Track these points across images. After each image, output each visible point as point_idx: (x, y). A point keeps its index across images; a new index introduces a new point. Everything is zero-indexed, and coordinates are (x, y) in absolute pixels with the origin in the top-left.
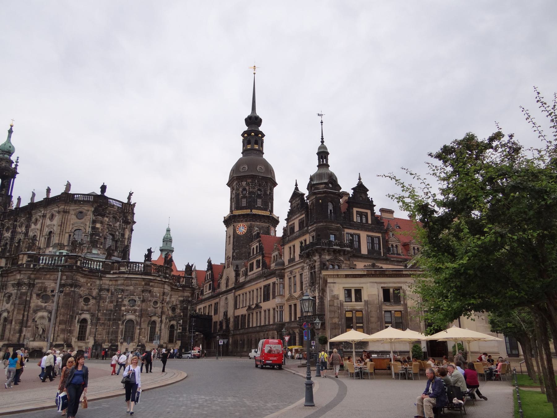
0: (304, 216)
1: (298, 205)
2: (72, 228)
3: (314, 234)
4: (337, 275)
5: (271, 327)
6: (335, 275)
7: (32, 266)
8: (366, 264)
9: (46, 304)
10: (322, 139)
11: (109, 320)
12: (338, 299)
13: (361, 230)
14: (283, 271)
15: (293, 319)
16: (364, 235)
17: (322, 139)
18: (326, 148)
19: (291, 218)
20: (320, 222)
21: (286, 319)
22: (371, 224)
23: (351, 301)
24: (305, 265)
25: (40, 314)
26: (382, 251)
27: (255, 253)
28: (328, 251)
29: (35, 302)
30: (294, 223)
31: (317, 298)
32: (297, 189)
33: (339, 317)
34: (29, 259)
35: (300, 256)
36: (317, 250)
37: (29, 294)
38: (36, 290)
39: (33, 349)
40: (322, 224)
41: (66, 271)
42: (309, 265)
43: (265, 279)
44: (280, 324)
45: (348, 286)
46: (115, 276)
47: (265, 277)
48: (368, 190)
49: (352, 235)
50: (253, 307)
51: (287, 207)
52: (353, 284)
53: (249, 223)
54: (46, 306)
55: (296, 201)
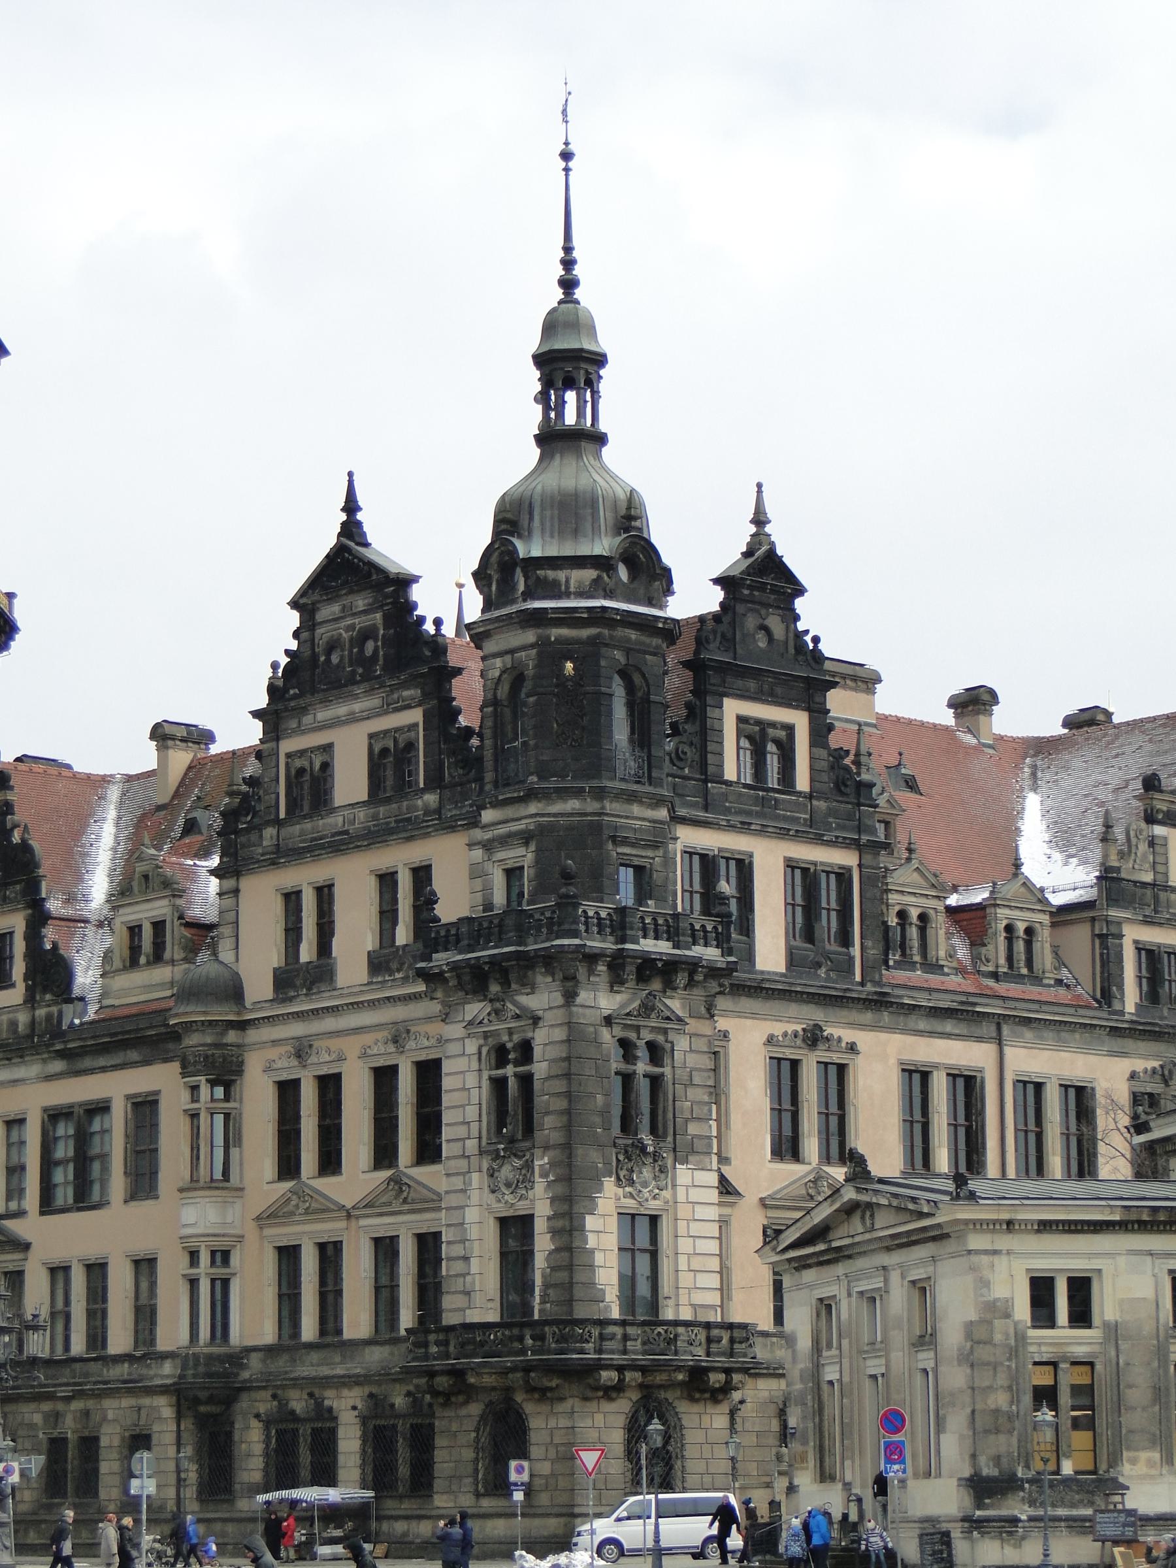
0: (415, 716)
1: (367, 634)
3: (524, 856)
4: (1009, 1223)
5: (123, 1370)
6: (1000, 1222)
8: (778, 1029)
10: (568, 263)
12: (1008, 1316)
13: (762, 832)
14: (232, 1037)
15: (309, 1329)
16: (770, 860)
17: (568, 263)
19: (304, 710)
20: (563, 793)
21: (254, 1321)
22: (810, 796)
23: (1052, 1324)
24: (455, 1030)
26: (856, 951)
28: (610, 967)
30: (328, 748)
31: (540, 1226)
32: (351, 529)
33: (1010, 1388)
36: (549, 960)
40: (573, 805)
42: (486, 1035)
43: (58, 1066)
44: (210, 1358)
45: (1043, 1265)
47: (63, 1055)
48: (800, 591)
49: (708, 864)
51: (277, 635)
52: (1063, 1257)
55: (347, 611)
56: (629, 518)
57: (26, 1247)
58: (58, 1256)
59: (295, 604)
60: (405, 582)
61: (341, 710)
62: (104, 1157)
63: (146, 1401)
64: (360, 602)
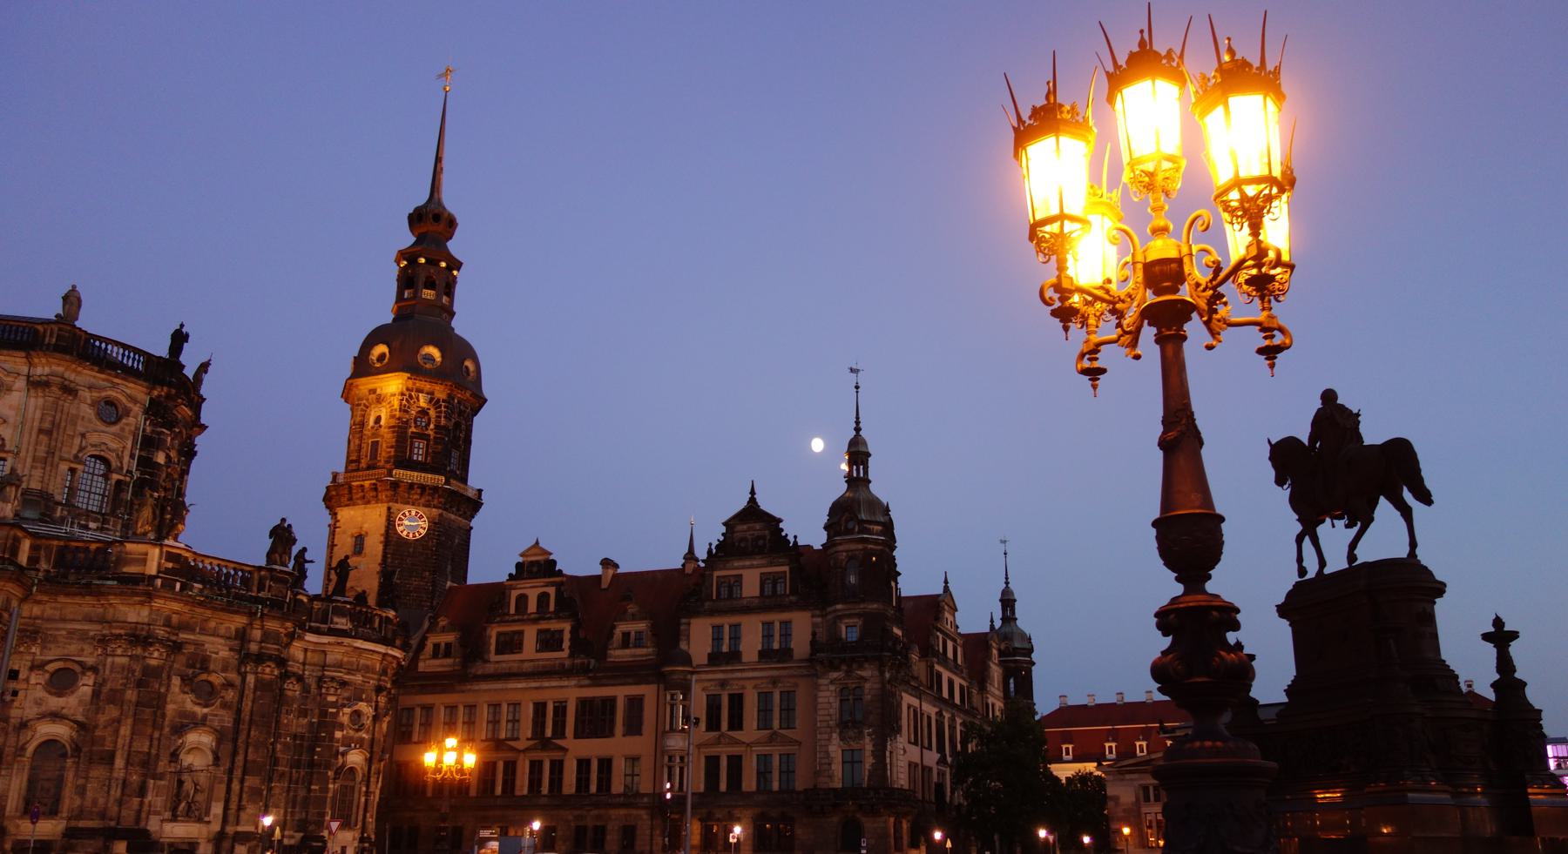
0: (786, 568)
1: (759, 538)
2: (81, 449)
7: (178, 586)
9: (205, 710)
10: (857, 423)
11: (296, 764)
17: (857, 423)
18: (865, 444)
25: (192, 738)
27: (532, 607)
29: (180, 700)
31: (868, 753)
32: (752, 500)
34: (170, 565)
35: (765, 654)
37: (164, 676)
38: (179, 662)
39: (171, 845)
41: (274, 618)
43: (587, 682)
46: (325, 639)
50: (521, 745)
53: (435, 512)
54: (205, 717)
56: (887, 510)
57: (565, 750)
58: (584, 754)
59: (725, 524)
60: (780, 521)
61: (747, 563)
62: (612, 721)
63: (634, 812)
64: (758, 526)
